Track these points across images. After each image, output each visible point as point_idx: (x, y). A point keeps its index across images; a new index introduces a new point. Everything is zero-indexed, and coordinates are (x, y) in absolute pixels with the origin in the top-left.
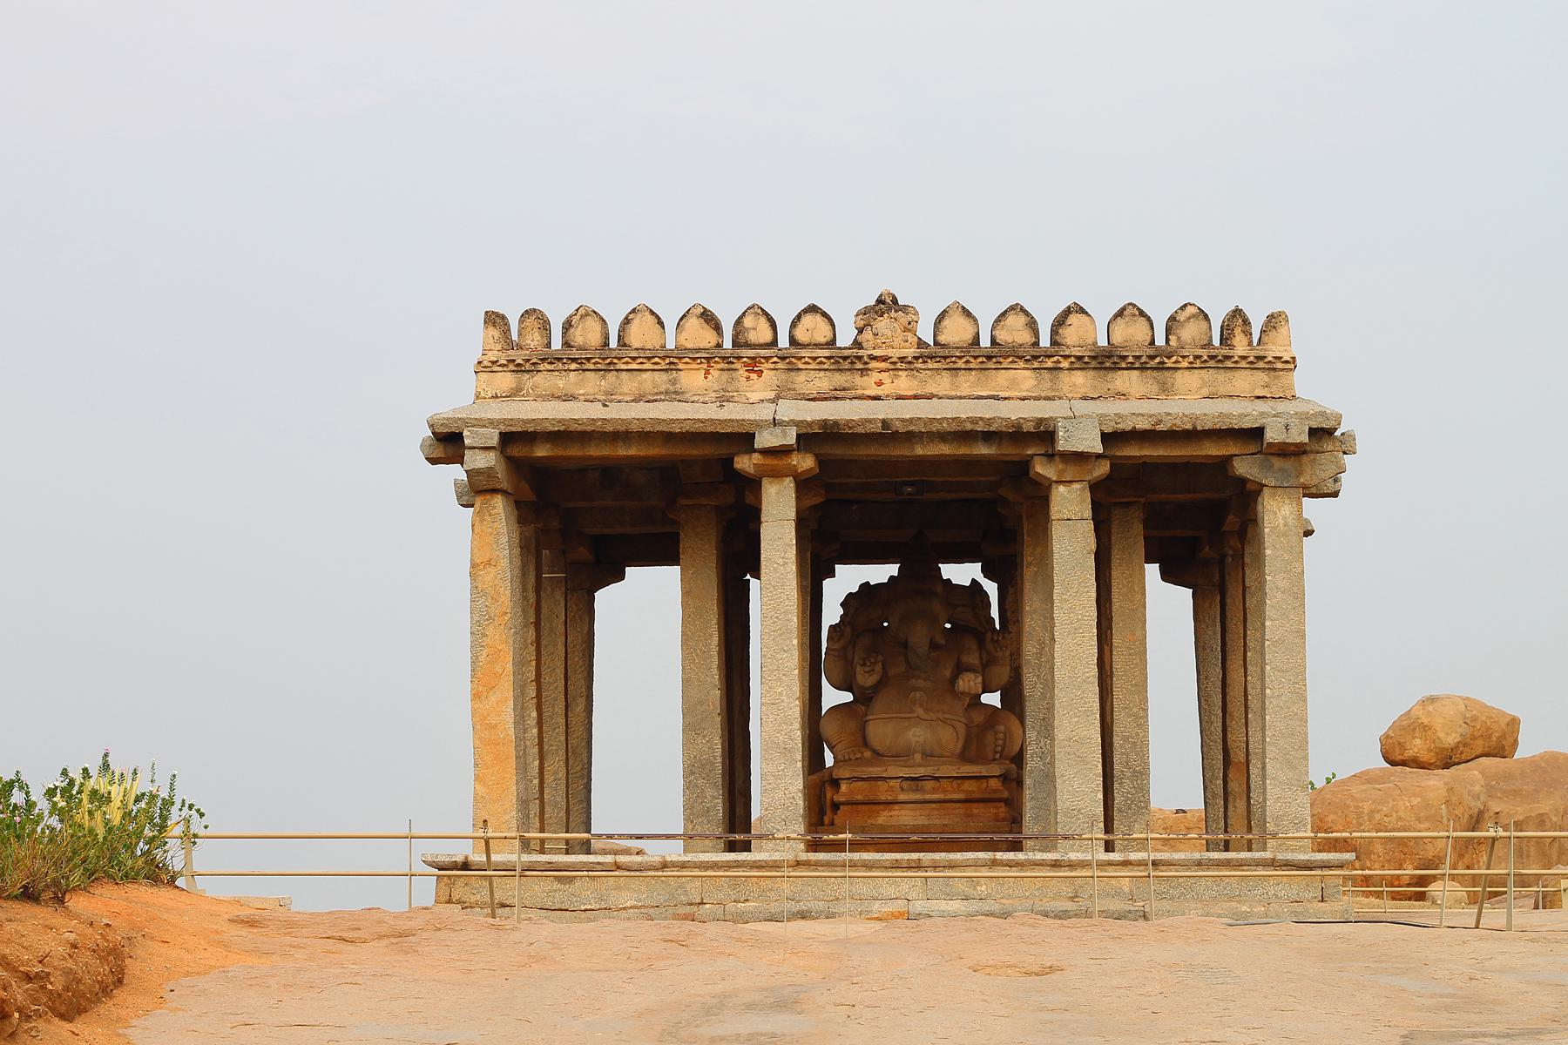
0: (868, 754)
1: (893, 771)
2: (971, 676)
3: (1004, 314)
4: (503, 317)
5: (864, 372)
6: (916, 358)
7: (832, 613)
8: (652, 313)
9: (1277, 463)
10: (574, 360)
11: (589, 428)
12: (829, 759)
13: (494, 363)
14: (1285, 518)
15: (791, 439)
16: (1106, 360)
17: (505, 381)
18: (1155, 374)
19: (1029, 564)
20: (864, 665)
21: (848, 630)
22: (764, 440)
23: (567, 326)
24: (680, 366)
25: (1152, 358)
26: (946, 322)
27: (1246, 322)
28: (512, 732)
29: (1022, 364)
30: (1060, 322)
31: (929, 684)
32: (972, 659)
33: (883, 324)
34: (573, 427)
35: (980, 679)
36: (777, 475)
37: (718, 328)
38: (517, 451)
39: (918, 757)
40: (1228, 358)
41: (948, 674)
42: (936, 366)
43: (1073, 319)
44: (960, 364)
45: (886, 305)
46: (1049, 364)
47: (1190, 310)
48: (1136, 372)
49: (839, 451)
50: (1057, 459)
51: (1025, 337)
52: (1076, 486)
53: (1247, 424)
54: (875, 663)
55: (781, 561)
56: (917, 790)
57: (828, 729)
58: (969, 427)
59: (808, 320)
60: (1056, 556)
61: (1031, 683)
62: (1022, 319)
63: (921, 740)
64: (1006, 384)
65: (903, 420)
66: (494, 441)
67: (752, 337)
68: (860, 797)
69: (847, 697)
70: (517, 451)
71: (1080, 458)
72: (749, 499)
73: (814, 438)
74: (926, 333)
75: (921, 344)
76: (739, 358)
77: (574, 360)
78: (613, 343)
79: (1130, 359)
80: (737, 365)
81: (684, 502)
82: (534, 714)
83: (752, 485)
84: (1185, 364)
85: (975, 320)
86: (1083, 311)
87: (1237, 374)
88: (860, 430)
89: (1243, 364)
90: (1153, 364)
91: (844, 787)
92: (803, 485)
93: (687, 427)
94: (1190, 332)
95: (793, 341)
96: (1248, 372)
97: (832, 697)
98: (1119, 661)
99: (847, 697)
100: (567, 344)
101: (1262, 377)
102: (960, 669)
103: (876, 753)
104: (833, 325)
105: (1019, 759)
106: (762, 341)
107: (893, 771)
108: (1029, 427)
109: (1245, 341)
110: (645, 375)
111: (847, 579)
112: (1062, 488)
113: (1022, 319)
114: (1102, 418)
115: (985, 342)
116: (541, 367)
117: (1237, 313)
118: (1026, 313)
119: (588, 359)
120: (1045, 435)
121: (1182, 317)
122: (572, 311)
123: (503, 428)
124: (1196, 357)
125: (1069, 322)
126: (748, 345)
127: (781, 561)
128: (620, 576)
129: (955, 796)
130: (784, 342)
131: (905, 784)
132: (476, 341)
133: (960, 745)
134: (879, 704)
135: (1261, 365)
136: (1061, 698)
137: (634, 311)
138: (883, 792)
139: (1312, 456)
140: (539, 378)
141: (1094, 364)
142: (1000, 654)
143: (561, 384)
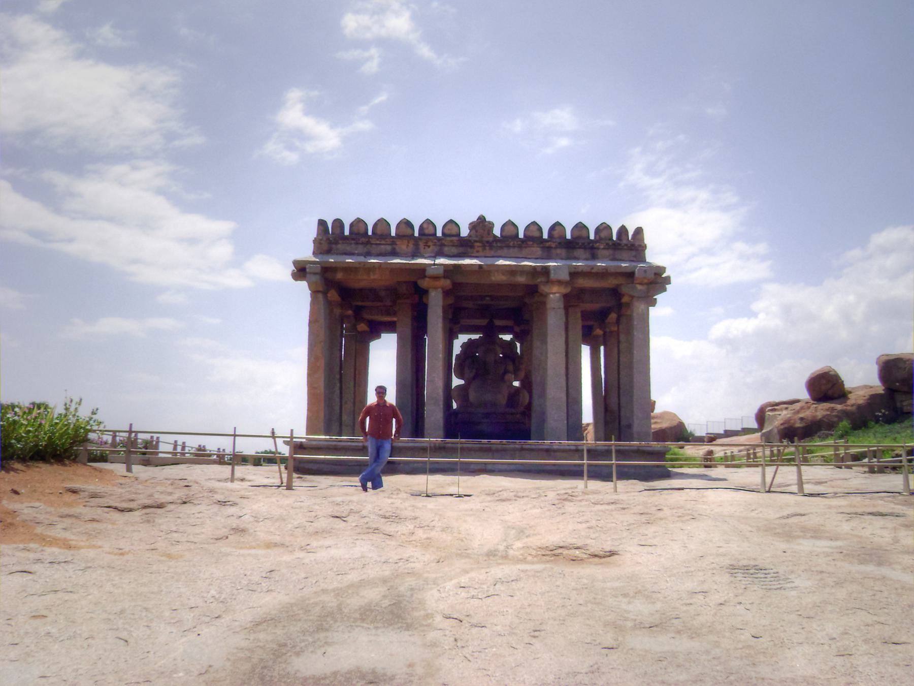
5: (472, 247)
7: (457, 349)
9: (639, 287)
12: (455, 406)
15: (441, 271)
22: (429, 272)
23: (352, 225)
26: (506, 228)
30: (552, 229)
36: (435, 288)
38: (329, 275)
40: (620, 244)
43: (557, 228)
45: (482, 219)
46: (547, 244)
49: (460, 279)
51: (536, 234)
53: (629, 270)
57: (454, 394)
61: (536, 378)
62: (536, 227)
66: (319, 270)
67: (426, 232)
70: (329, 275)
71: (560, 283)
72: (424, 300)
73: (450, 271)
75: (495, 236)
83: (425, 292)
86: (560, 224)
92: (446, 293)
95: (443, 233)
98: (571, 370)
99: (462, 382)
101: (633, 253)
102: (506, 372)
105: (529, 407)
108: (539, 270)
111: (462, 339)
114: (570, 266)
120: (546, 271)
124: (607, 244)
128: (379, 337)
136: (550, 383)
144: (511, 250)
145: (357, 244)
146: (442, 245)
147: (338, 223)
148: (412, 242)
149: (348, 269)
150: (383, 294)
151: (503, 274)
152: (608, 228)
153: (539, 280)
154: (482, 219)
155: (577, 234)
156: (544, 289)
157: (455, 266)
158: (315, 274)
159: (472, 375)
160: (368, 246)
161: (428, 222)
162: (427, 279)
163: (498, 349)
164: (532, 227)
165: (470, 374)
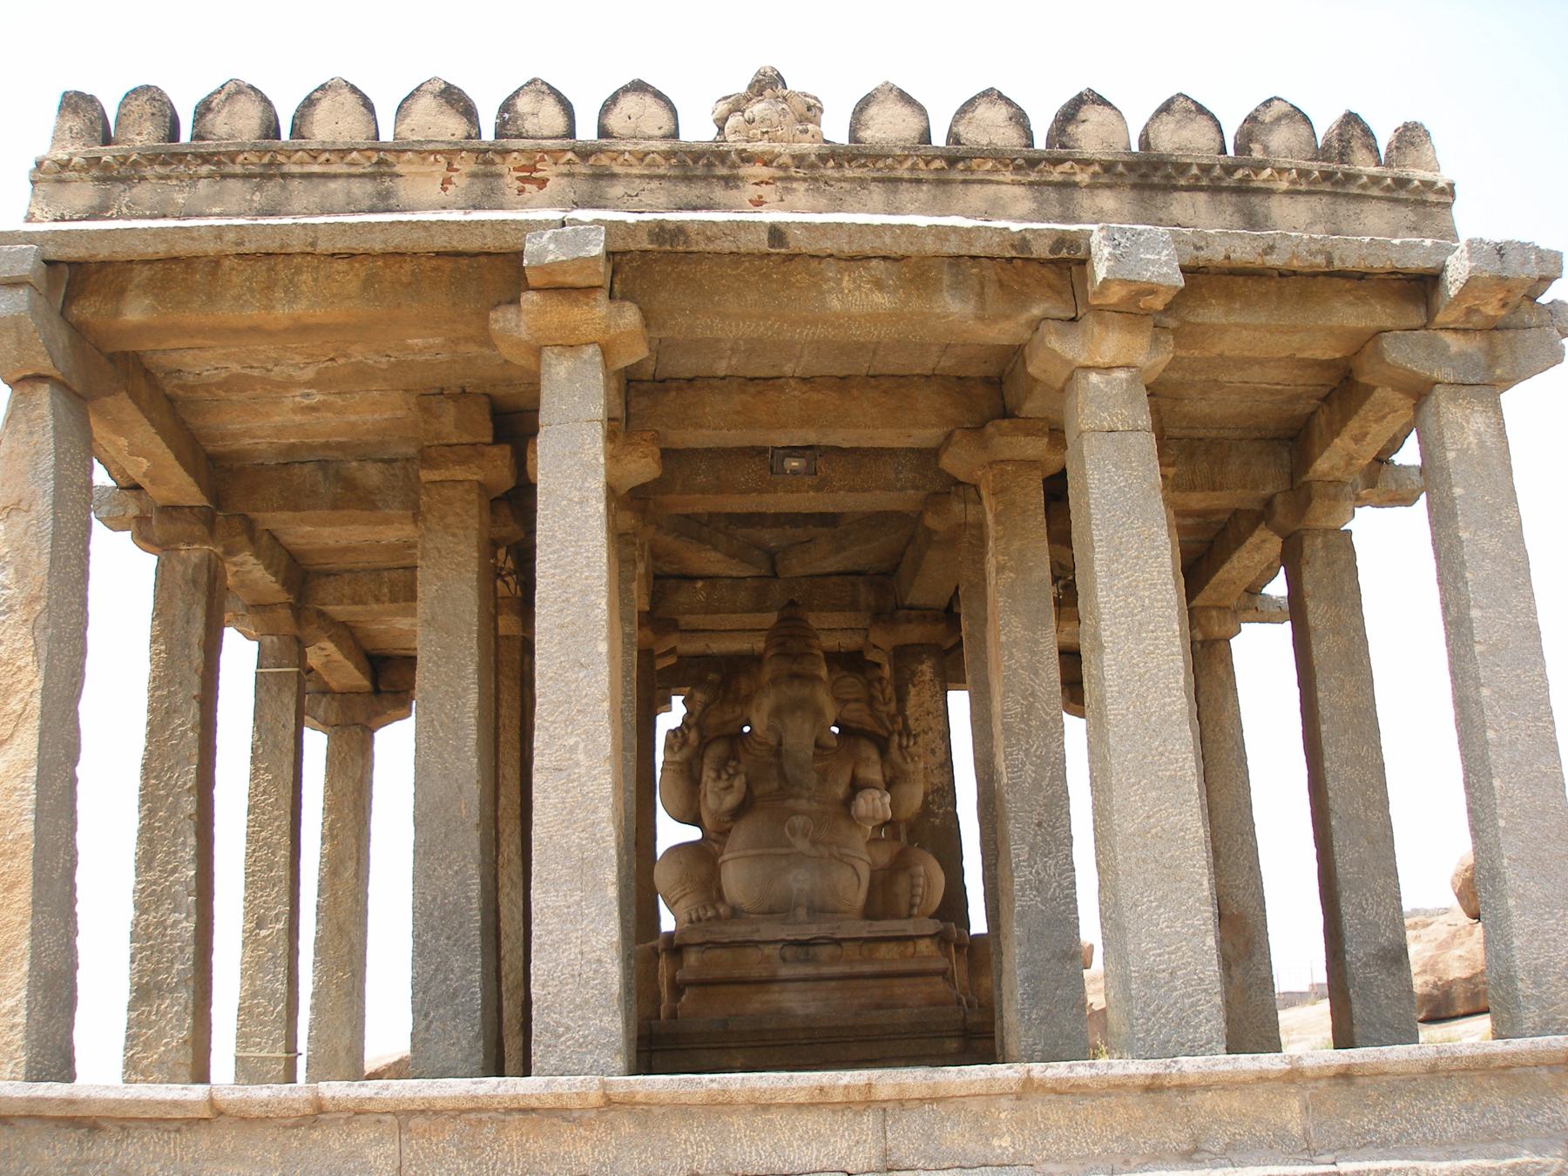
1: (768, 931)
2: (877, 794)
3: (970, 104)
4: (91, 100)
5: (731, 181)
6: (823, 158)
7: (672, 717)
8: (354, 90)
9: (1455, 343)
10: (205, 158)
11: (211, 248)
12: (668, 923)
13: (64, 165)
14: (1478, 434)
16: (1148, 175)
17: (84, 193)
18: (1234, 198)
19: (1001, 569)
21: (693, 736)
22: (542, 250)
24: (398, 169)
25: (1229, 170)
26: (873, 110)
27: (1367, 132)
28: (28, 828)
29: (1009, 177)
30: (1070, 114)
31: (815, 806)
33: (757, 109)
34: (183, 248)
35: (888, 799)
36: (571, 347)
37: (468, 111)
38: (86, 310)
39: (802, 913)
40: (1350, 178)
41: (840, 791)
42: (858, 173)
43: (1091, 113)
44: (902, 171)
45: (767, 83)
46: (1056, 175)
47: (1278, 108)
48: (1202, 197)
50: (1090, 321)
51: (1007, 137)
52: (1122, 375)
54: (737, 773)
56: (807, 960)
58: (930, 246)
59: (629, 103)
60: (1094, 493)
62: (1000, 113)
64: (983, 206)
65: (807, 227)
67: (529, 125)
68: (718, 973)
69: (693, 834)
74: (835, 129)
76: (505, 152)
77: (205, 158)
78: (285, 134)
79: (1195, 171)
80: (502, 168)
81: (426, 475)
82: (192, 841)
84: (1284, 185)
85: (922, 110)
87: (1366, 206)
88: (726, 246)
89: (1375, 192)
90: (1229, 182)
91: (692, 958)
93: (396, 241)
94: (1281, 139)
95: (603, 132)
96: (1385, 206)
97: (671, 833)
99: (693, 834)
100: (197, 136)
101: (1407, 215)
102: (856, 787)
103: (736, 913)
104: (673, 110)
106: (546, 133)
107: (768, 931)
108: (1041, 250)
109: (1368, 157)
110: (333, 185)
112: (1094, 378)
113: (1000, 113)
115: (939, 139)
116: (148, 172)
117: (1351, 119)
118: (1009, 102)
119: (232, 156)
121: (1267, 117)
122: (217, 86)
123: (52, 252)
125: (1081, 116)
126: (520, 136)
127: (576, 495)
129: (866, 968)
130: (587, 131)
131: (788, 952)
132: (39, 134)
133: (862, 895)
134: (741, 834)
135: (1403, 194)
137: (322, 87)
138: (752, 963)
139: (1510, 334)
140: (142, 192)
141: (1133, 178)
142: (910, 767)
143: (180, 198)
144: (906, 194)
145: (224, 177)
146: (603, 176)
147: (150, 99)
148: (466, 165)
149: (177, 270)
150: (372, 475)
151: (879, 285)
152: (1297, 116)
153: (1036, 311)
154: (767, 83)
155: (1168, 140)
156: (1065, 347)
157: (660, 232)
158: (14, 284)
159: (730, 800)
160: (272, 188)
161: (541, 88)
162: (529, 298)
163: (824, 698)
164: (983, 111)
165: (718, 797)
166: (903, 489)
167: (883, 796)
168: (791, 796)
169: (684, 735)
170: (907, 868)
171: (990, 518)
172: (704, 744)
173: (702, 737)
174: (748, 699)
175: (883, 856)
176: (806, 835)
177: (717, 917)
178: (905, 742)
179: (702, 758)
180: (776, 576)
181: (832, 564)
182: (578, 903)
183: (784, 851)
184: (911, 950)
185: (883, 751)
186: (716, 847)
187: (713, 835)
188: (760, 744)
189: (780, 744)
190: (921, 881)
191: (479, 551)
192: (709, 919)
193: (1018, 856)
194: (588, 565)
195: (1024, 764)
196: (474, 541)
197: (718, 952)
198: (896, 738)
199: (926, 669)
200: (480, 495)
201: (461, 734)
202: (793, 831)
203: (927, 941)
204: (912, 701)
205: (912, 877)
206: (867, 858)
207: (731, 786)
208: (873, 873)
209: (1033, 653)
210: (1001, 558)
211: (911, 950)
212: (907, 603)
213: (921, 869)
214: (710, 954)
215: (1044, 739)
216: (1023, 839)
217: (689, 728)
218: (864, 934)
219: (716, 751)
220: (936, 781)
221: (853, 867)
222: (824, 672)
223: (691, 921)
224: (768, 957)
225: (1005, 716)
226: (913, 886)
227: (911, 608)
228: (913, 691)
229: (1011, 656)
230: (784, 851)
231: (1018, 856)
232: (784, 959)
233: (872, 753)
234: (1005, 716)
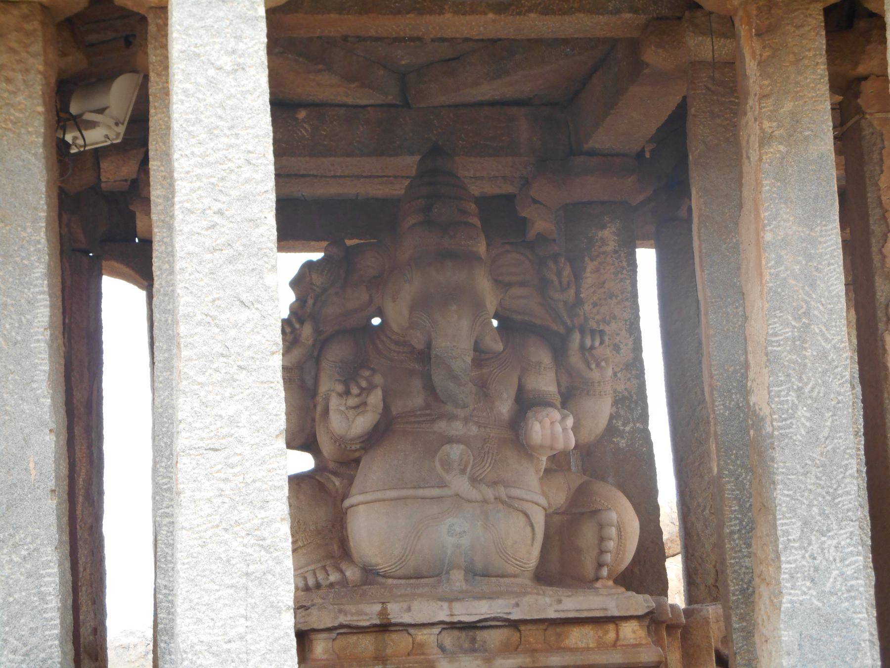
0: (352, 573)
2: (556, 415)
19: (766, 140)
20: (347, 393)
21: (307, 331)
31: (474, 430)
32: (546, 383)
35: (570, 422)
41: (505, 408)
54: (372, 387)
55: (226, 62)
63: (465, 541)
69: (304, 462)
102: (526, 403)
127: (226, 62)
131: (448, 639)
133: (532, 555)
142: (595, 375)
159: (362, 424)
163: (484, 284)
166: (617, 11)
167: (564, 418)
168: (441, 416)
169: (294, 330)
170: (595, 513)
171: (751, 67)
172: (322, 343)
173: (317, 332)
174: (378, 282)
175: (559, 495)
176: (463, 471)
177: (344, 582)
178: (588, 343)
179: (318, 360)
180: (406, 105)
181: (488, 91)
182: (242, 638)
183: (435, 492)
184: (612, 635)
185: (559, 353)
186: (337, 482)
187: (331, 465)
188: (396, 343)
189: (429, 346)
190: (613, 531)
191: (45, 104)
192: (332, 585)
193: (787, 533)
194: (248, 162)
195: (795, 407)
196: (38, 89)
197: (353, 639)
198: (576, 337)
199: (609, 235)
200: (43, 24)
201: (26, 364)
202: (447, 465)
203: (633, 625)
204: (589, 279)
205: (601, 526)
206: (543, 501)
207: (365, 404)
208: (547, 516)
209: (810, 257)
210: (766, 124)
211: (612, 635)
212: (586, 146)
213: (613, 516)
214: (342, 642)
215: (824, 373)
216: (793, 510)
217: (302, 322)
218: (552, 615)
219: (337, 353)
220: (621, 387)
221: (526, 515)
222: (481, 248)
223: (307, 589)
224: (421, 645)
225: (770, 343)
226: (602, 539)
227: (591, 153)
228: (590, 266)
229: (779, 261)
230: (435, 492)
231: (787, 533)
232: (442, 648)
233: (544, 357)
234: (770, 343)
